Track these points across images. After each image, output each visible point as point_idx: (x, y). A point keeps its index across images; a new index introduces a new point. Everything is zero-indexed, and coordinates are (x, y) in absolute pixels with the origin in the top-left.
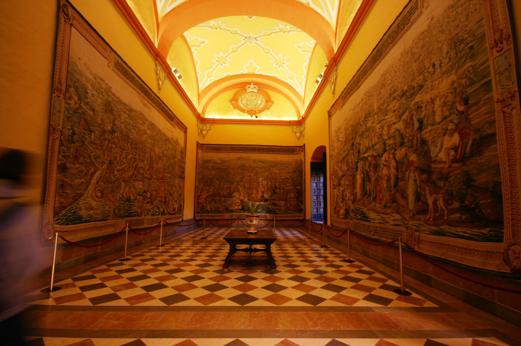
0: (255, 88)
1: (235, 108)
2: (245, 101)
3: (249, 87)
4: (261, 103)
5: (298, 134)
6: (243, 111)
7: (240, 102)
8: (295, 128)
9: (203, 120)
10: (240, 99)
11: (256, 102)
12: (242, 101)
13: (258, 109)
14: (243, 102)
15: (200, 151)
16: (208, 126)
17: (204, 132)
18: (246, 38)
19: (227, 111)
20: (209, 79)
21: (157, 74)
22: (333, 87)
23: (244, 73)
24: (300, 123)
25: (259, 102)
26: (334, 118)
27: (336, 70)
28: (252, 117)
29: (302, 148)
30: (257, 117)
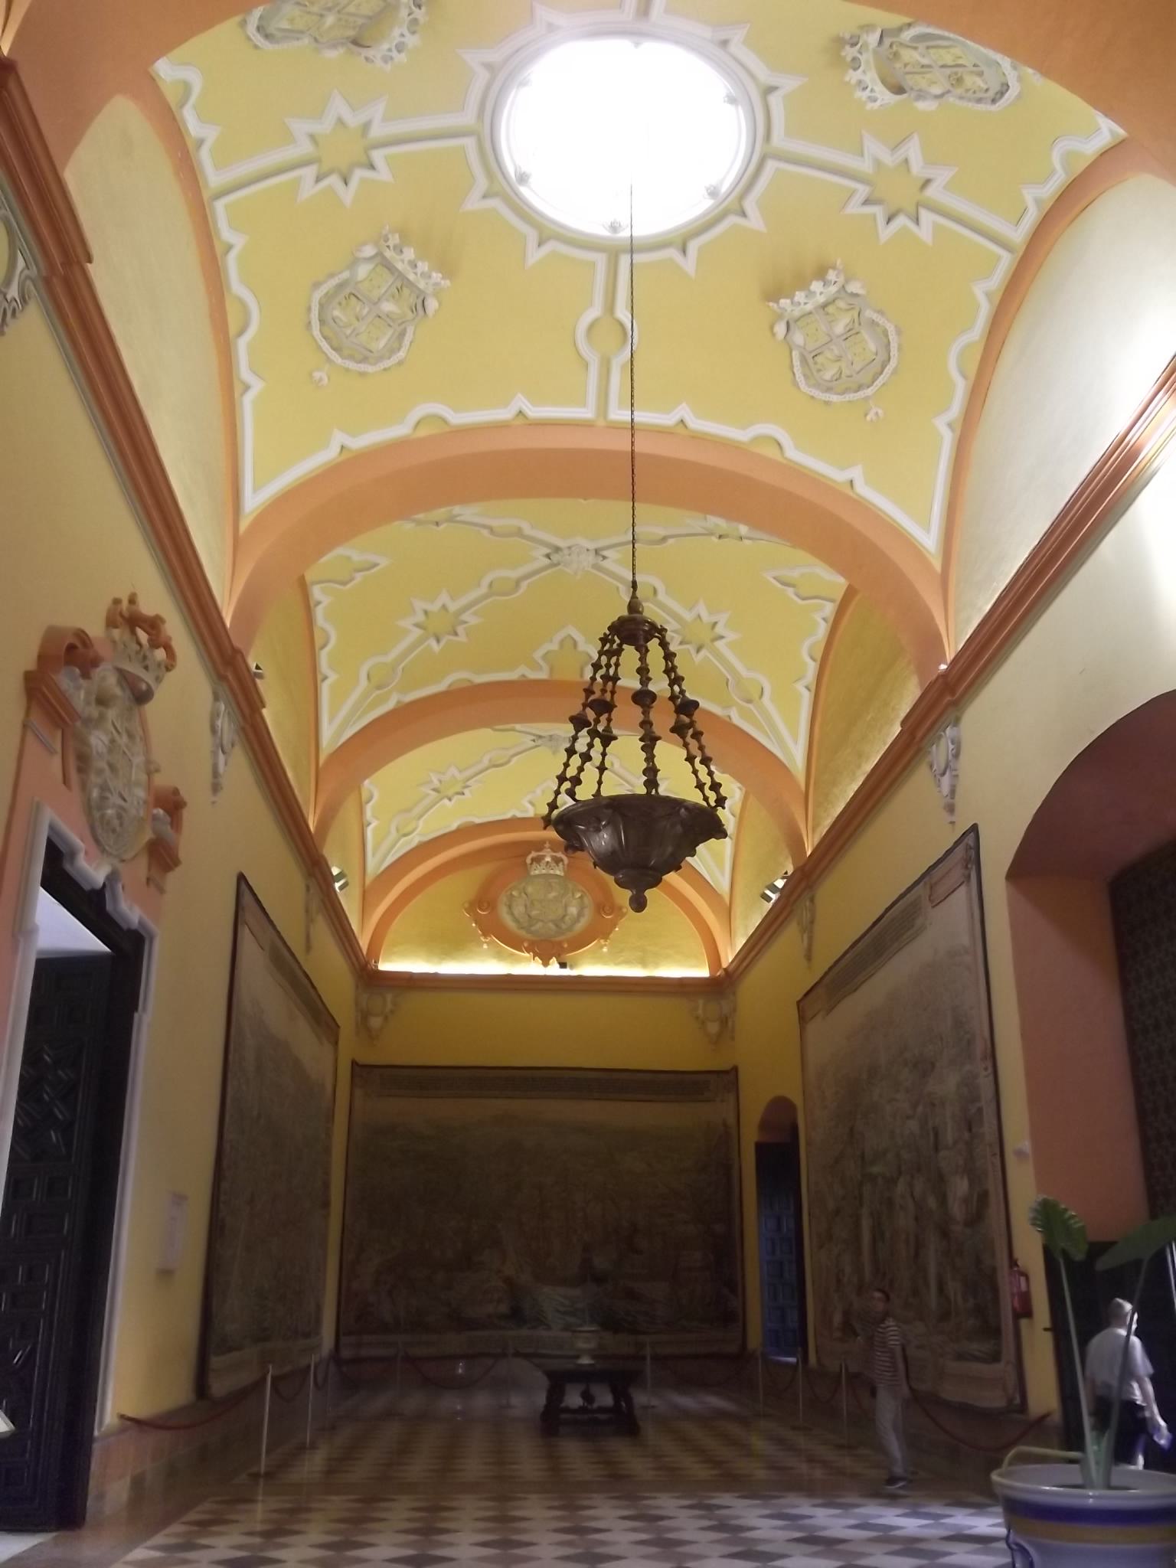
0: (557, 861)
1: (485, 935)
2: (522, 909)
3: (538, 860)
4: (580, 915)
5: (713, 1028)
6: (515, 943)
7: (503, 912)
8: (701, 1002)
9: (370, 979)
10: (503, 898)
11: (560, 912)
12: (510, 907)
13: (569, 935)
14: (516, 912)
15: (358, 1092)
16: (389, 997)
17: (375, 1022)
18: (540, 737)
19: (453, 946)
20: (403, 840)
21: (307, 911)
22: (805, 936)
23: (519, 815)
24: (720, 986)
25: (573, 910)
26: (812, 1027)
27: (812, 900)
28: (546, 964)
29: (728, 1079)
30: (563, 965)
